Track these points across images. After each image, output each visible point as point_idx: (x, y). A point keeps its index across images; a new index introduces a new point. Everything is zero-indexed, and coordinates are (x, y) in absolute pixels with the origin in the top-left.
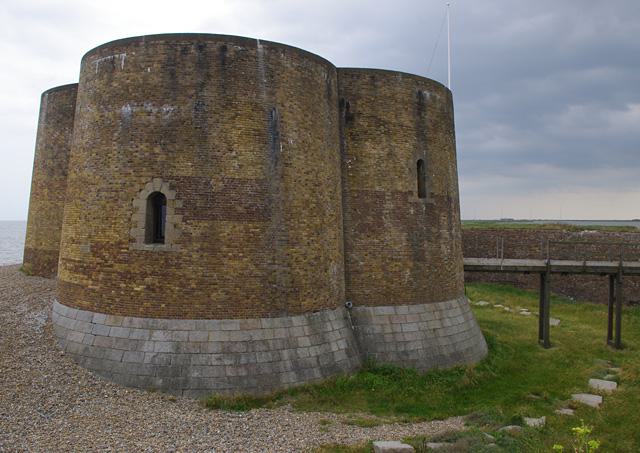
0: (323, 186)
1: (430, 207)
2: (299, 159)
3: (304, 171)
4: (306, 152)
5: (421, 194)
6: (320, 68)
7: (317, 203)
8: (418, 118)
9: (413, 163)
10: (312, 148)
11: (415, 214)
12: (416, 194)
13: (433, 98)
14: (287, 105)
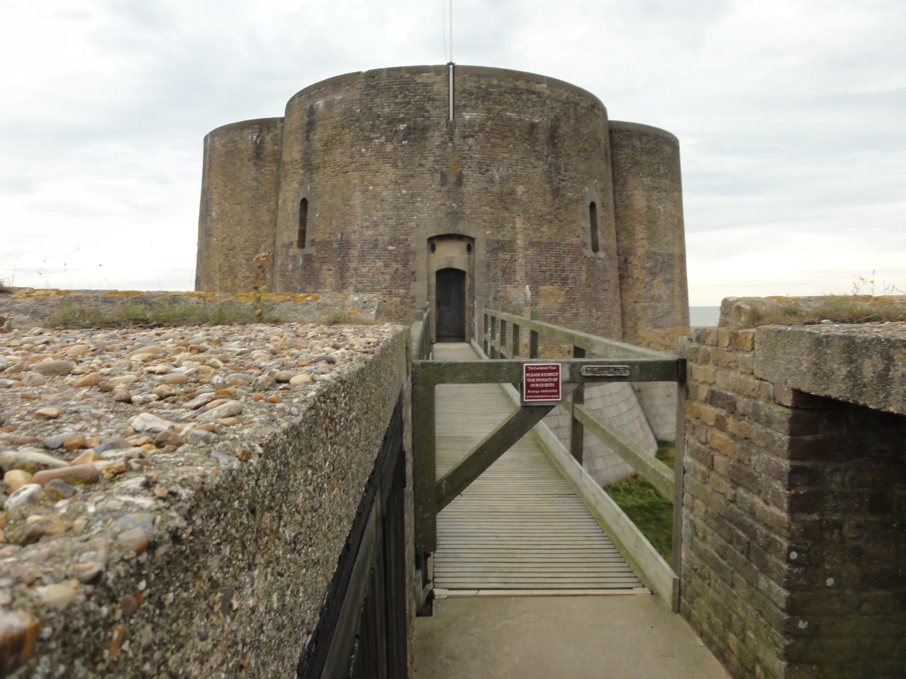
0: (237, 250)
1: (308, 259)
2: (217, 228)
3: (220, 238)
4: (223, 221)
5: (301, 244)
6: (246, 132)
7: (230, 267)
8: (306, 143)
9: (296, 206)
10: (229, 215)
11: (293, 270)
12: (295, 244)
13: (329, 106)
14: (214, 182)
